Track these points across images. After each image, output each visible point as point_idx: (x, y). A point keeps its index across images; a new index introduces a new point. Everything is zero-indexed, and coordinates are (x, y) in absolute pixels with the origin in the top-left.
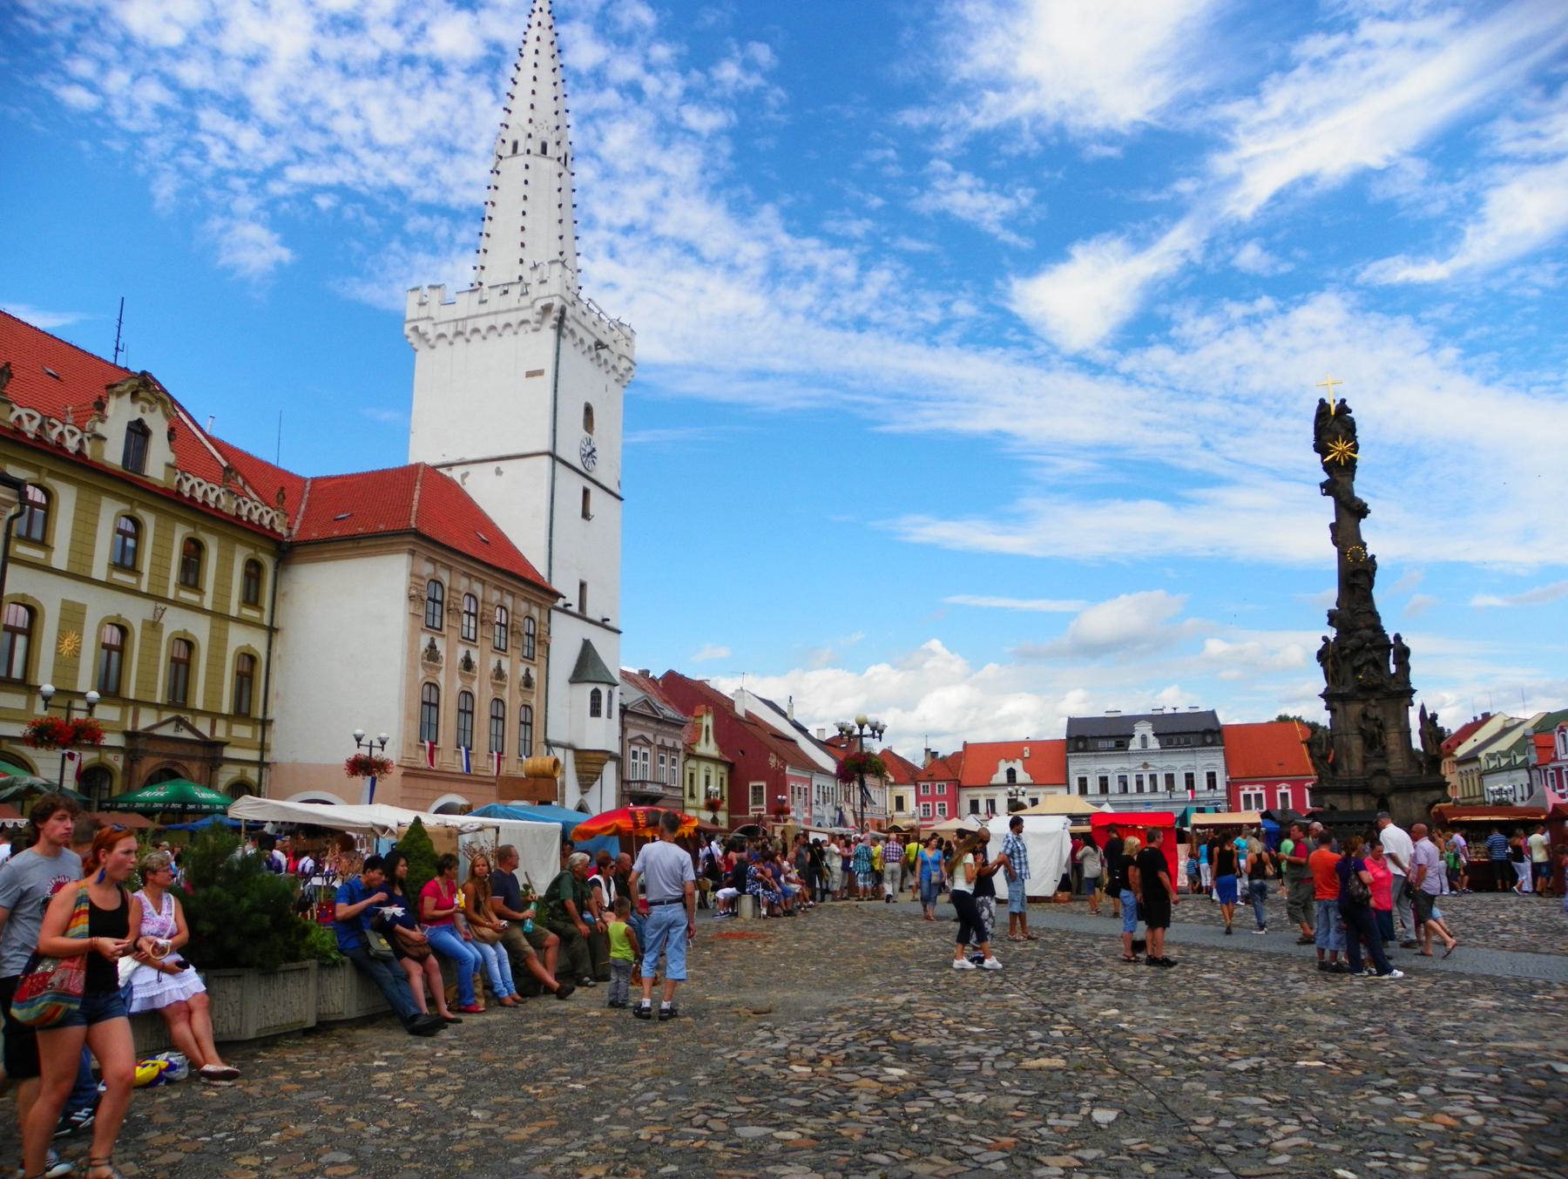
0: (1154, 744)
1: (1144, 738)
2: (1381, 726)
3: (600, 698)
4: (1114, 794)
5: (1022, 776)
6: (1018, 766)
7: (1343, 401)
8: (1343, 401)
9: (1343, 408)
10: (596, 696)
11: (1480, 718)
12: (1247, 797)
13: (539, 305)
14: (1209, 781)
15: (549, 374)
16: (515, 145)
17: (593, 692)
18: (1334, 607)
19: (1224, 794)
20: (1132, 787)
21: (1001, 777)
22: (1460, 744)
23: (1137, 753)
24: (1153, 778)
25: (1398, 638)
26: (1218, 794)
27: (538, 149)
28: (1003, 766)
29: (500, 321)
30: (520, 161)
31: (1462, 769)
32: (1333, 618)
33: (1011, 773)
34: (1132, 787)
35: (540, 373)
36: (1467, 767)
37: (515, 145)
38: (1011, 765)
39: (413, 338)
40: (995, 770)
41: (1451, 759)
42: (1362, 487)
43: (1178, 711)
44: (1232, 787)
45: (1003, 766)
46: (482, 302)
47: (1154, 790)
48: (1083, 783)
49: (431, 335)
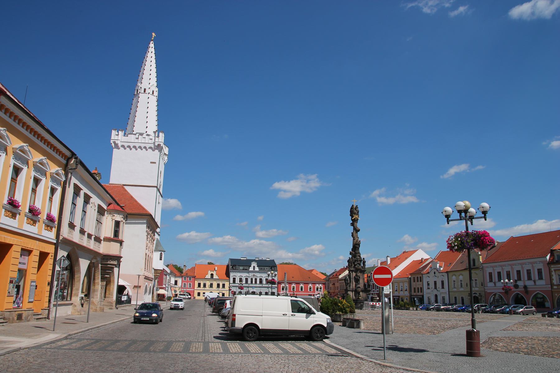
0: (257, 269)
1: (254, 267)
2: (360, 278)
3: (162, 255)
5: (215, 277)
6: (214, 273)
7: (357, 206)
8: (357, 206)
9: (357, 207)
10: (161, 255)
11: (346, 267)
13: (156, 144)
14: (260, 281)
15: (157, 163)
16: (145, 90)
17: (160, 254)
18: (351, 251)
20: (249, 281)
21: (209, 276)
22: (340, 274)
24: (256, 279)
25: (364, 259)
27: (151, 93)
28: (210, 273)
29: (143, 145)
30: (147, 96)
32: (351, 254)
33: (212, 275)
34: (249, 281)
35: (155, 163)
37: (145, 90)
38: (212, 272)
39: (113, 145)
42: (359, 225)
43: (263, 259)
46: (138, 138)
47: (256, 282)
48: (234, 279)
49: (120, 145)
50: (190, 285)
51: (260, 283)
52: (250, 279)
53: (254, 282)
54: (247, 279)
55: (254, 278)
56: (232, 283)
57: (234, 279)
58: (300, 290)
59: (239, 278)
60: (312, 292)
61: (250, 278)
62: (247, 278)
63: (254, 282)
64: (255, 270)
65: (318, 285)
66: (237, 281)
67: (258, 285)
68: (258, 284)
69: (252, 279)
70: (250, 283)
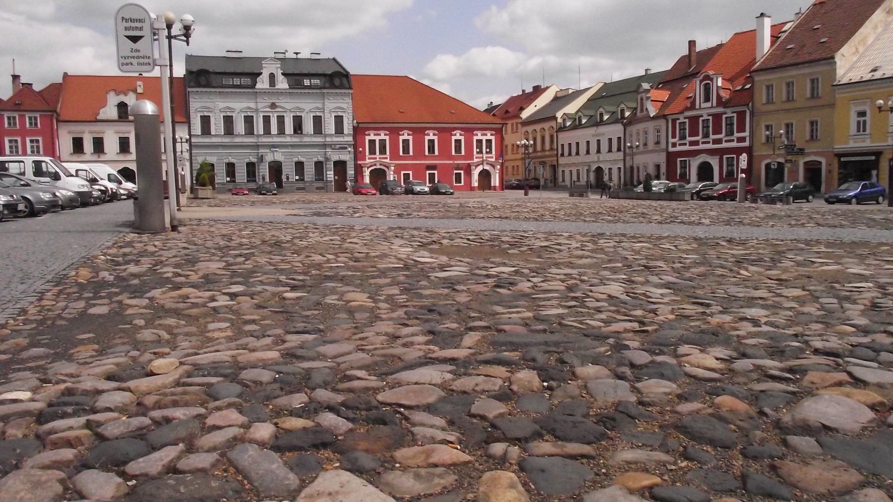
0: (282, 84)
1: (272, 77)
4: (239, 135)
12: (372, 142)
19: (351, 139)
20: (259, 128)
21: (110, 111)
22: (522, 109)
23: (264, 93)
24: (281, 120)
26: (347, 139)
28: (113, 100)
31: (530, 129)
34: (259, 128)
36: (538, 127)
40: (104, 104)
41: (515, 121)
43: (299, 56)
44: (358, 131)
45: (113, 100)
47: (281, 131)
48: (206, 121)
50: (35, 144)
51: (295, 132)
52: (261, 120)
53: (274, 129)
54: (249, 120)
55: (275, 115)
56: (200, 134)
57: (206, 121)
58: (427, 153)
59: (222, 115)
60: (464, 158)
61: (261, 115)
62: (250, 114)
63: (274, 129)
64: (277, 87)
65: (483, 135)
66: (218, 126)
67: (288, 139)
68: (290, 136)
69: (267, 120)
70: (262, 132)
